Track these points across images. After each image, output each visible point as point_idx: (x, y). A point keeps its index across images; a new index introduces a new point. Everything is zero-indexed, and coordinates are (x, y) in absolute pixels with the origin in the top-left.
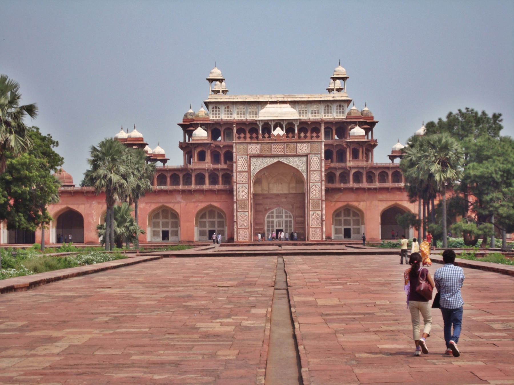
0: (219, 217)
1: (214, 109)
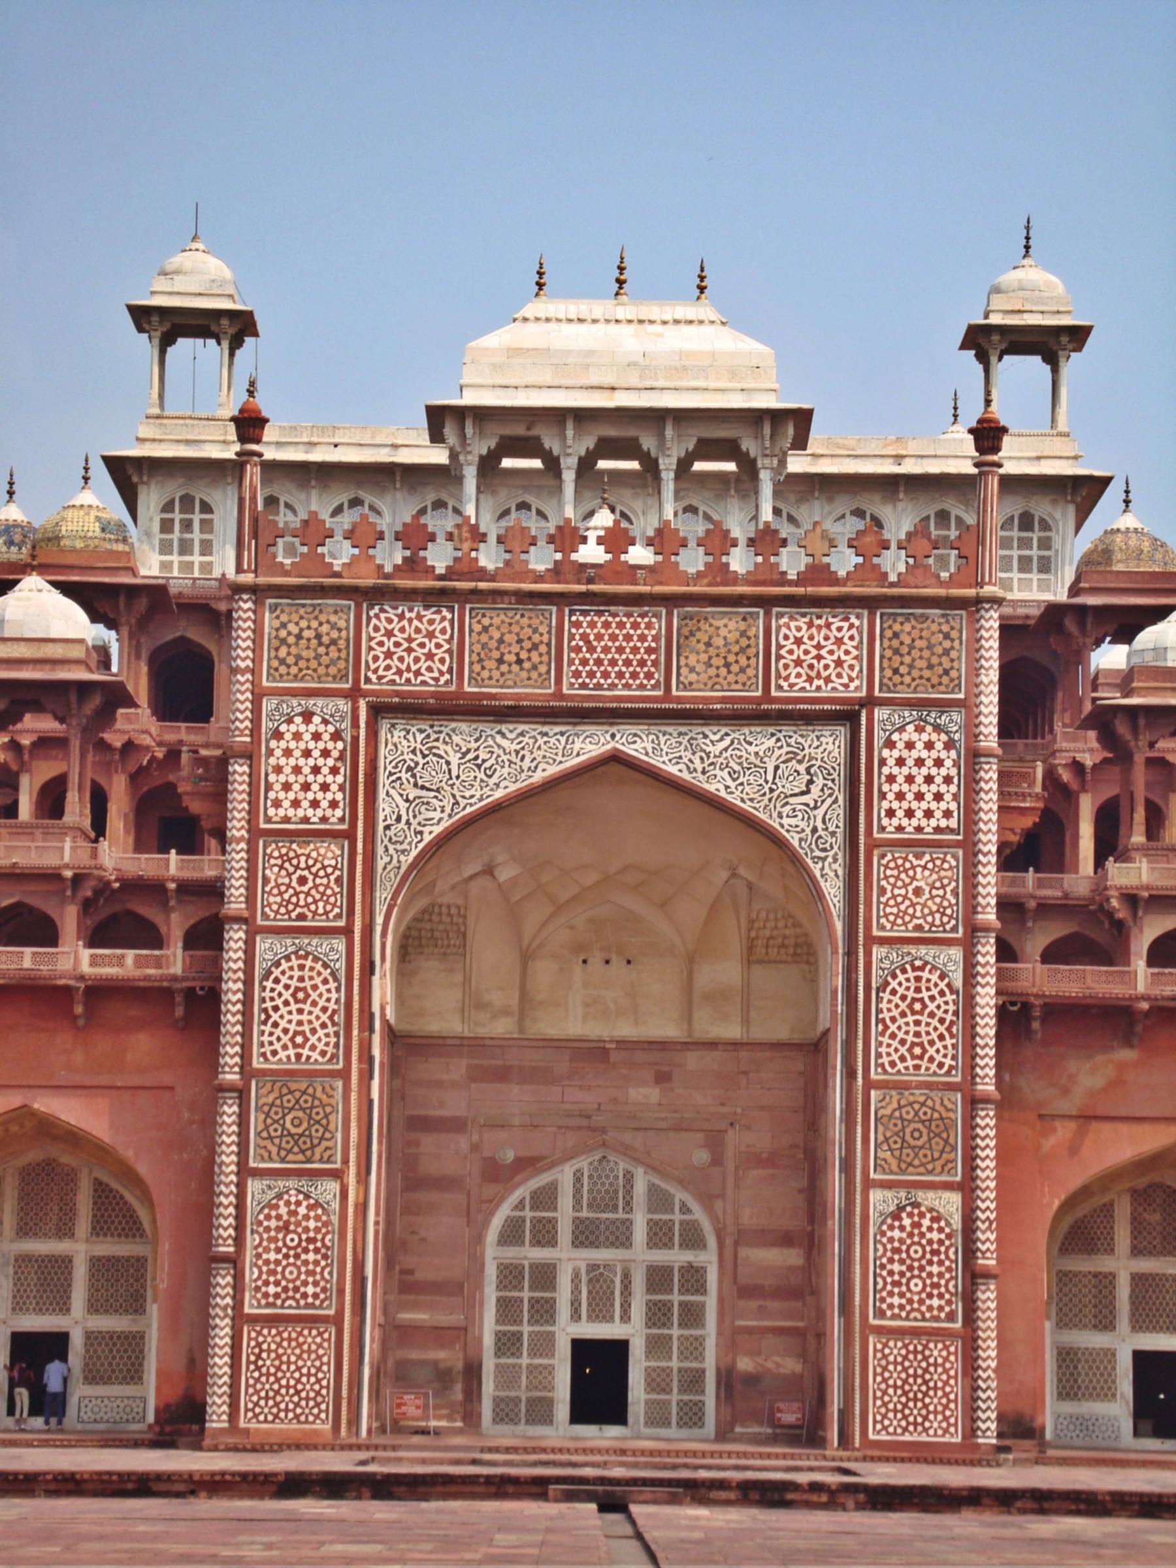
0: (99, 1228)
1: (177, 516)
